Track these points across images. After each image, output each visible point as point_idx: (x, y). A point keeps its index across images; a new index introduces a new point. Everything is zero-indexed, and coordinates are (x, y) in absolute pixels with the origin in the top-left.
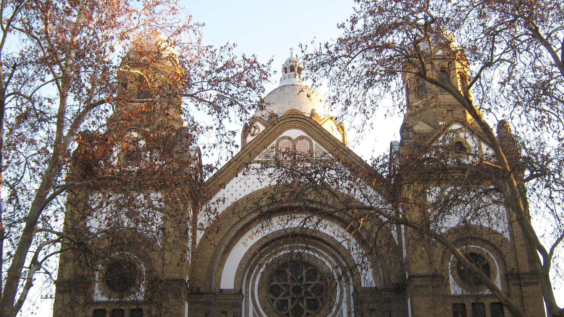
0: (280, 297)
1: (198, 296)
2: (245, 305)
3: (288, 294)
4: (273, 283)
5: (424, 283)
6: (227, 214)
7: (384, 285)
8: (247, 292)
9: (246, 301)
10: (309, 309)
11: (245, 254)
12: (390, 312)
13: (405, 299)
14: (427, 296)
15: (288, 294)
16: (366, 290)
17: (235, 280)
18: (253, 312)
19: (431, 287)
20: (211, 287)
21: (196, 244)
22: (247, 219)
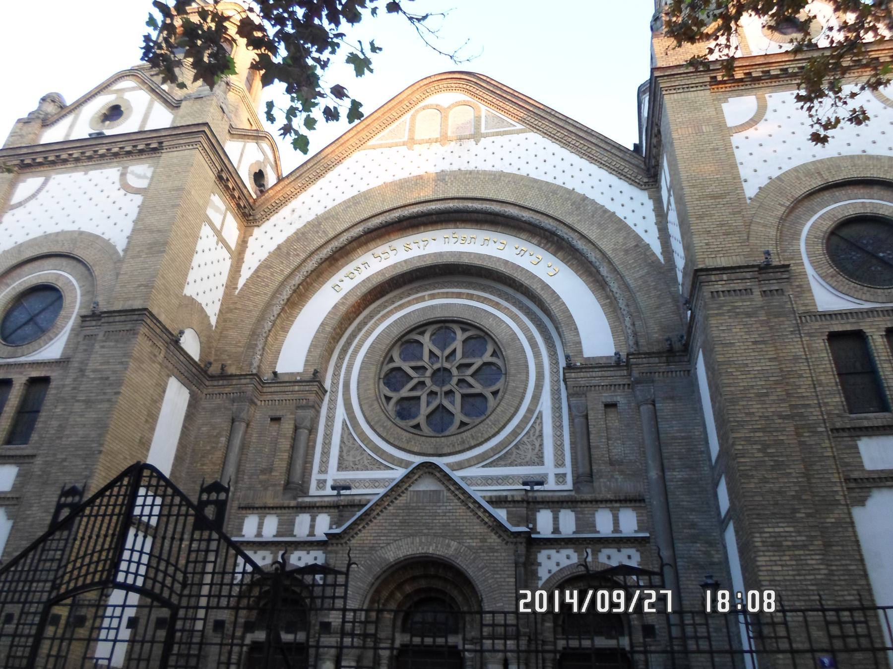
1: (221, 382)
2: (329, 409)
3: (422, 384)
4: (392, 365)
6: (303, 234)
7: (637, 343)
8: (335, 384)
9: (331, 400)
10: (466, 415)
11: (335, 307)
12: (653, 403)
13: (689, 371)
14: (749, 315)
15: (422, 384)
17: (307, 356)
18: (344, 422)
19: (757, 292)
20: (251, 364)
21: (236, 288)
22: (341, 240)
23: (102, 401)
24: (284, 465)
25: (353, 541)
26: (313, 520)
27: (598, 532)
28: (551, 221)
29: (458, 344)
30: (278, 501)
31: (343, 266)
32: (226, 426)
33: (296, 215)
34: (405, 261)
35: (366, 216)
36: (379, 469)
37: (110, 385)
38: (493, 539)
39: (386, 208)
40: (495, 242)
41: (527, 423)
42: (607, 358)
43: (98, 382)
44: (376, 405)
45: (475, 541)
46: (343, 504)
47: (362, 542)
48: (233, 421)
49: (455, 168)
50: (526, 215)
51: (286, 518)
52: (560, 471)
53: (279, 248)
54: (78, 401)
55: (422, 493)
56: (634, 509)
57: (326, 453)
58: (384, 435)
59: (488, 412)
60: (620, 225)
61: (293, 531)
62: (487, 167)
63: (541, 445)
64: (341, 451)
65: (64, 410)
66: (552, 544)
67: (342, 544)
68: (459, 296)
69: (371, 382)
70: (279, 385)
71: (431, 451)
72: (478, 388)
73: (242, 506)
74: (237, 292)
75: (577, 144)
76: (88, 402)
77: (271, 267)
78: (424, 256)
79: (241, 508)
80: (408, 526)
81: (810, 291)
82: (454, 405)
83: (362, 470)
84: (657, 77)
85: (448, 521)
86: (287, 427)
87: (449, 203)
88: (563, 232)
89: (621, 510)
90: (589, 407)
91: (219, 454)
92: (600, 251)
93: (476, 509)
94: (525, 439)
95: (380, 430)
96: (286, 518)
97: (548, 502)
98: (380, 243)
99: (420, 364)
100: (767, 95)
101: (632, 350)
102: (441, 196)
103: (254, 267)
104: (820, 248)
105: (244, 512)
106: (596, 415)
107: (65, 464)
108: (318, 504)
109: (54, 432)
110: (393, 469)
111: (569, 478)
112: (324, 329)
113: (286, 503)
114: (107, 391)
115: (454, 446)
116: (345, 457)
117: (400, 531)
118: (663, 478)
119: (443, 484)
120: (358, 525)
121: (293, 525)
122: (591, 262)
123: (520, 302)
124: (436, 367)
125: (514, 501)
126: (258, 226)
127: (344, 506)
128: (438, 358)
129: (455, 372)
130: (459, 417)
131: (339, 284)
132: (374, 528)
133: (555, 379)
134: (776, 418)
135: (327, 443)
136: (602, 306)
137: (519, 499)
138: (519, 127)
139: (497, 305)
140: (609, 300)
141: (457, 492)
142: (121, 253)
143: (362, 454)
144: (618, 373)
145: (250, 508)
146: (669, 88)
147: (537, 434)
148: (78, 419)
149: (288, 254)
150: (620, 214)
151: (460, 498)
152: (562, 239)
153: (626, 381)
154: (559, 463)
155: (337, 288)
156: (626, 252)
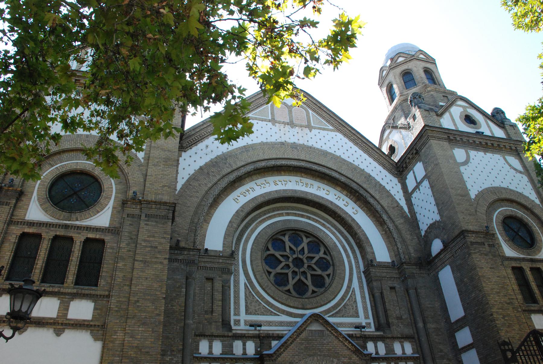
0: (278, 270)
1: (176, 252)
3: (288, 266)
4: (268, 253)
5: (479, 240)
7: (405, 257)
11: (237, 212)
14: (486, 255)
16: (382, 265)
18: (245, 284)
22: (241, 171)
23: (156, 263)
24: (220, 309)
25: (279, 359)
26: (244, 345)
27: (396, 354)
28: (355, 184)
29: (304, 245)
30: (220, 332)
31: (239, 187)
32: (184, 281)
33: (209, 149)
34: (276, 191)
35: (254, 160)
36: (271, 315)
37: (159, 252)
38: (355, 358)
39: (266, 158)
40: (324, 190)
41: (348, 294)
42: (388, 263)
43: (149, 249)
44: (264, 276)
45: (346, 359)
46: (263, 335)
47: (284, 359)
48: (187, 278)
49: (301, 142)
50: (343, 179)
51: (227, 343)
52: (368, 321)
53: (201, 168)
54: (137, 260)
55: (314, 332)
56: (410, 342)
57: (237, 303)
58: (272, 295)
59: (327, 285)
60: (388, 194)
61: (232, 351)
62: (318, 146)
63: (356, 306)
64: (246, 303)
65: (125, 265)
66: (376, 360)
67: (272, 360)
68: (302, 216)
69: (260, 261)
70: (209, 257)
71: (300, 306)
72: (319, 272)
73: (197, 334)
74: (177, 192)
75: (362, 145)
76: (145, 262)
77: (198, 180)
78: (286, 190)
79: (196, 335)
80: (309, 350)
81: (502, 246)
82: (293, 280)
83: (261, 315)
84: (426, 130)
85: (331, 348)
86: (218, 285)
87: (301, 163)
88: (362, 192)
89: (405, 342)
90: (383, 288)
91: (183, 299)
92: (382, 206)
93: (343, 341)
94: (348, 303)
95: (269, 291)
96: (227, 343)
97: (371, 338)
98: (259, 177)
99: (285, 253)
100: (469, 151)
101: (404, 261)
102: (296, 157)
103: (187, 177)
104: (501, 228)
105: (198, 338)
106: (387, 294)
107: (138, 304)
108: (246, 335)
109: (121, 280)
110: (279, 315)
111: (372, 325)
112: (232, 225)
113: (226, 334)
114: (158, 256)
115: (312, 304)
116: (249, 306)
117: (305, 353)
118: (424, 327)
119: (324, 326)
120: (281, 349)
121: (232, 347)
122: (377, 211)
123: (335, 225)
124: (295, 256)
125: (356, 337)
126: (185, 151)
127: (263, 337)
128: (294, 251)
129: (305, 261)
130: (311, 288)
131: (238, 198)
132: (290, 351)
133: (359, 271)
134: (504, 303)
135: (237, 297)
136: (382, 235)
137: (359, 336)
138: (331, 127)
139: (323, 225)
140: (384, 232)
141: (332, 332)
142: (142, 161)
143: (259, 305)
144: (394, 272)
145: (203, 336)
146: (432, 137)
147: (354, 300)
148: (141, 274)
149: (208, 173)
150: (388, 187)
151: (334, 335)
152: (362, 195)
153: (398, 276)
154: (367, 317)
155: (236, 200)
156: (393, 208)
